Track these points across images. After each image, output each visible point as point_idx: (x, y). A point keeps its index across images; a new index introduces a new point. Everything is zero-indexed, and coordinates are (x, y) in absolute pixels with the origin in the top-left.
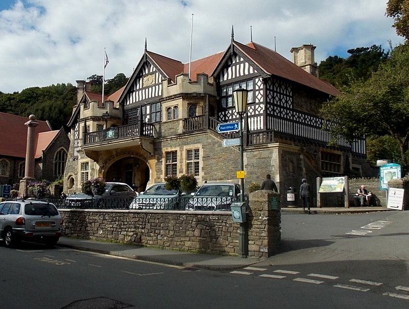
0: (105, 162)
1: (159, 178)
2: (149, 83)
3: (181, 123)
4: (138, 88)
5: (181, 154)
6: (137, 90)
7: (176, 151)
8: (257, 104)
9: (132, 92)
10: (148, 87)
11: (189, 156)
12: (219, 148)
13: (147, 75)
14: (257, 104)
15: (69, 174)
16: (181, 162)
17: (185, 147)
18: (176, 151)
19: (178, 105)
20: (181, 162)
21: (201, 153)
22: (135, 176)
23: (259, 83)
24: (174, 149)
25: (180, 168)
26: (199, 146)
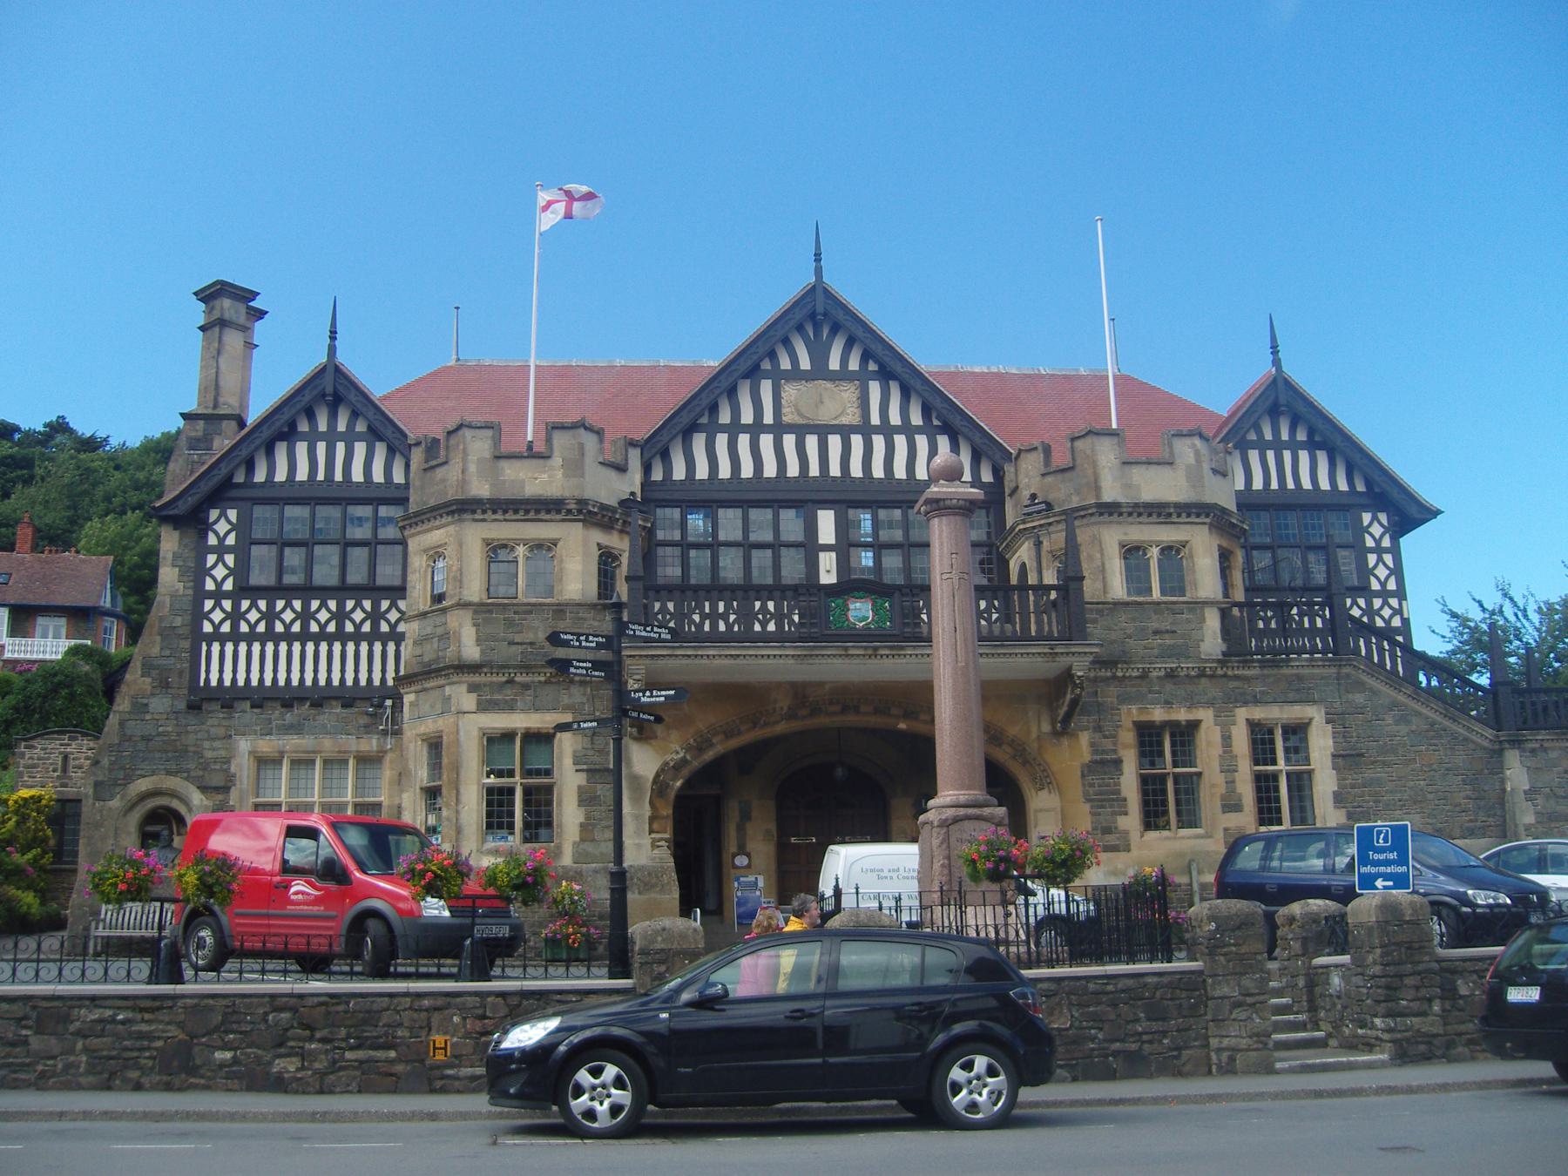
0: (700, 747)
1: (1107, 830)
2: (826, 415)
3: (1213, 621)
4: (747, 417)
5: (1227, 740)
6: (735, 429)
7: (1194, 725)
8: (1377, 594)
9: (712, 430)
10: (801, 431)
11: (1262, 747)
12: (1403, 729)
13: (796, 375)
14: (1377, 594)
15: (143, 785)
16: (1229, 769)
17: (1242, 714)
18: (1194, 725)
19: (1184, 544)
20: (1229, 769)
21: (1321, 743)
22: (745, 816)
23: (1377, 530)
24: (1182, 715)
25: (1222, 789)
26: (1315, 714)
